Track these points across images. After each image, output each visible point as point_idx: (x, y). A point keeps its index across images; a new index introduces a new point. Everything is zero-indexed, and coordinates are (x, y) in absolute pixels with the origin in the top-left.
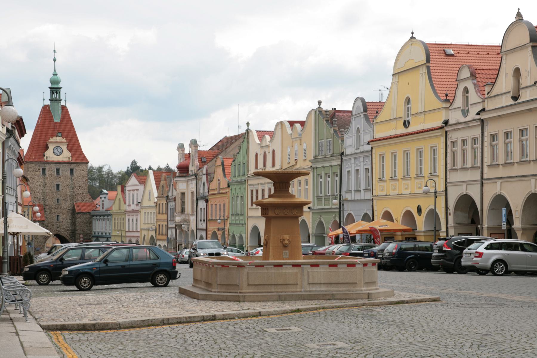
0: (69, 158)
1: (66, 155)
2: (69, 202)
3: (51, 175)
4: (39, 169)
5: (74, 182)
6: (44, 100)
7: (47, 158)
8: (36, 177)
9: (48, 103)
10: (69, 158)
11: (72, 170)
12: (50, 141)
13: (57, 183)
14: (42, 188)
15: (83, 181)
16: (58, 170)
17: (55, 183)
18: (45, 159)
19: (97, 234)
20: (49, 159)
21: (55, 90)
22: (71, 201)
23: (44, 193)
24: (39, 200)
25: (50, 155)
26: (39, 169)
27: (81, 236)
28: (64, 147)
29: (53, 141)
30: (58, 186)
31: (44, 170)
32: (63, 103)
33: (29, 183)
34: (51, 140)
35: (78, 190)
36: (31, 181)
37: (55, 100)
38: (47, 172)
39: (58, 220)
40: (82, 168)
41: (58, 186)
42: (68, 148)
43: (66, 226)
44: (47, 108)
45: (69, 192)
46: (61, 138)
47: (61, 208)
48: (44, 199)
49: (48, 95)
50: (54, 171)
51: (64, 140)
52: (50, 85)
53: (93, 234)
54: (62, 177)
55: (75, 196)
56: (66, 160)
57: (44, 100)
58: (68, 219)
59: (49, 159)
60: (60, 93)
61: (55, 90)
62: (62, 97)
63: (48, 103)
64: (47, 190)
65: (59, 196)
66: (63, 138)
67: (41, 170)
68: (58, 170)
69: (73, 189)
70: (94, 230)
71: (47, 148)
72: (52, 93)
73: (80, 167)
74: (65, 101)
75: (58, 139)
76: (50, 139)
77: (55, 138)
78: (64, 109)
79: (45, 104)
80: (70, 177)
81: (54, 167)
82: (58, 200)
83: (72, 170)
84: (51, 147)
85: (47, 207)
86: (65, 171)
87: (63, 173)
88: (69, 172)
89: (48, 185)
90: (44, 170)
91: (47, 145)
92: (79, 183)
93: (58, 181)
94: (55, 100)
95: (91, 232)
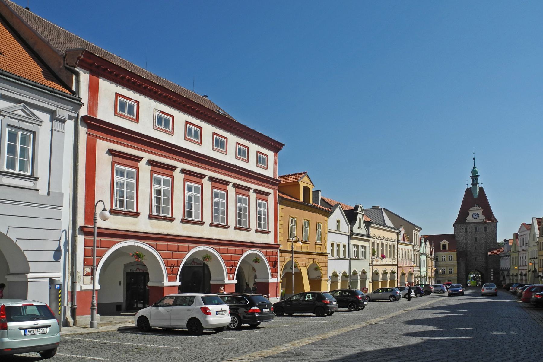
0: (484, 220)
1: (482, 218)
2: (483, 248)
3: (471, 232)
4: (463, 228)
5: (487, 235)
6: (467, 185)
7: (468, 220)
8: (461, 233)
9: (470, 186)
10: (484, 220)
11: (485, 228)
12: (470, 210)
13: (476, 237)
14: (465, 240)
15: (494, 234)
16: (476, 229)
17: (474, 237)
18: (467, 222)
19: (502, 269)
20: (469, 222)
21: (475, 177)
22: (485, 248)
23: (466, 243)
24: (463, 248)
25: (470, 218)
26: (463, 228)
27: (492, 270)
28: (480, 212)
29: (473, 209)
30: (476, 238)
31: (466, 229)
32: (480, 185)
33: (456, 238)
34: (471, 209)
35: (490, 240)
36: (457, 237)
37: (474, 184)
38: (468, 230)
39: (476, 261)
40: (493, 226)
41: (476, 238)
42: (483, 213)
43: (482, 264)
44: (469, 189)
45: (483, 241)
46: (478, 207)
47: (478, 252)
48: (466, 248)
49: (470, 181)
50: (473, 229)
51: (480, 208)
52: (471, 175)
53: (501, 269)
54: (479, 233)
55: (489, 245)
56: (481, 221)
57: (467, 185)
58: (483, 260)
59: (470, 221)
60: (478, 179)
61: (475, 177)
62: (480, 181)
63: (470, 186)
64: (468, 242)
65: (476, 245)
66: (479, 207)
67: (464, 229)
68: (476, 229)
69: (487, 240)
70: (501, 266)
71: (468, 214)
72: (473, 180)
73: (492, 225)
74: (482, 184)
75: (476, 208)
76: (470, 209)
77: (473, 208)
78: (481, 189)
79: (468, 187)
80: (484, 232)
81: (472, 225)
82: (476, 248)
83: (485, 228)
84: (471, 213)
85: (469, 252)
86: (481, 229)
87: (479, 229)
88: (484, 229)
89: (469, 238)
90: (466, 229)
91: (469, 212)
92: (491, 236)
93: (476, 235)
94: (474, 184)
95: (500, 267)
